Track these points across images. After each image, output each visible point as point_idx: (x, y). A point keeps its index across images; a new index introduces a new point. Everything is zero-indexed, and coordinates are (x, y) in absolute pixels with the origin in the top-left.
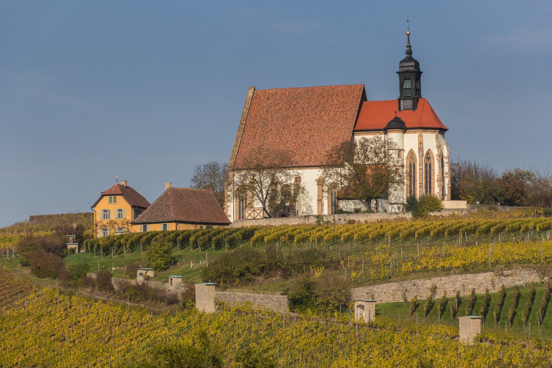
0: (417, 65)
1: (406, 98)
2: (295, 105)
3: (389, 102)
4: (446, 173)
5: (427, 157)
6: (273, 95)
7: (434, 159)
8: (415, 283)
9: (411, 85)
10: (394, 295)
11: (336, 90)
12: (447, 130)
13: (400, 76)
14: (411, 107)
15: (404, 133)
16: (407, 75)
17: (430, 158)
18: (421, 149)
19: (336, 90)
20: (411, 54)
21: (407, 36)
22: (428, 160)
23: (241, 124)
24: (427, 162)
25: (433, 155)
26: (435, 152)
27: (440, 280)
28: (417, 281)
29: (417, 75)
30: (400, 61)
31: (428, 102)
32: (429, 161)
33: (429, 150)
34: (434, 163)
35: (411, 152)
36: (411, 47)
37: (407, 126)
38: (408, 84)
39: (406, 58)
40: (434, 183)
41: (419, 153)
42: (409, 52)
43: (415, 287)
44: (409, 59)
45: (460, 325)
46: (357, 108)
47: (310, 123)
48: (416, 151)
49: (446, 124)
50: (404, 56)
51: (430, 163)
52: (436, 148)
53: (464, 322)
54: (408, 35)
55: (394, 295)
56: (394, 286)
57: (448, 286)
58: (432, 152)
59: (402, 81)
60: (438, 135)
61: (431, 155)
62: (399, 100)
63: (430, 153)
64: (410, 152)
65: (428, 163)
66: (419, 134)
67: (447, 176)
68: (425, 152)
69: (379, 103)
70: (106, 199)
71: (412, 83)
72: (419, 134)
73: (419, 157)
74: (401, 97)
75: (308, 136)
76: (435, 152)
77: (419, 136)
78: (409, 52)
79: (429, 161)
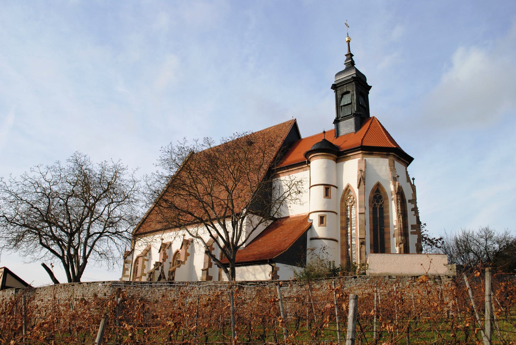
4: (412, 226)
5: (375, 197)
7: (387, 198)
13: (336, 92)
14: (353, 130)
15: (337, 161)
17: (380, 197)
18: (362, 180)
20: (352, 63)
21: (347, 44)
22: (378, 202)
24: (375, 205)
25: (385, 193)
26: (391, 188)
30: (336, 74)
31: (379, 122)
32: (380, 204)
33: (378, 185)
34: (388, 206)
35: (348, 190)
36: (352, 55)
39: (346, 68)
40: (389, 239)
41: (358, 188)
42: (351, 64)
51: (381, 205)
54: (349, 41)
58: (383, 188)
59: (338, 97)
60: (394, 162)
61: (382, 194)
63: (380, 189)
64: (346, 189)
65: (378, 207)
66: (359, 159)
67: (415, 230)
68: (371, 185)
71: (353, 95)
72: (359, 159)
73: (359, 194)
74: (337, 118)
76: (391, 188)
77: (359, 162)
78: (351, 64)
79: (380, 204)
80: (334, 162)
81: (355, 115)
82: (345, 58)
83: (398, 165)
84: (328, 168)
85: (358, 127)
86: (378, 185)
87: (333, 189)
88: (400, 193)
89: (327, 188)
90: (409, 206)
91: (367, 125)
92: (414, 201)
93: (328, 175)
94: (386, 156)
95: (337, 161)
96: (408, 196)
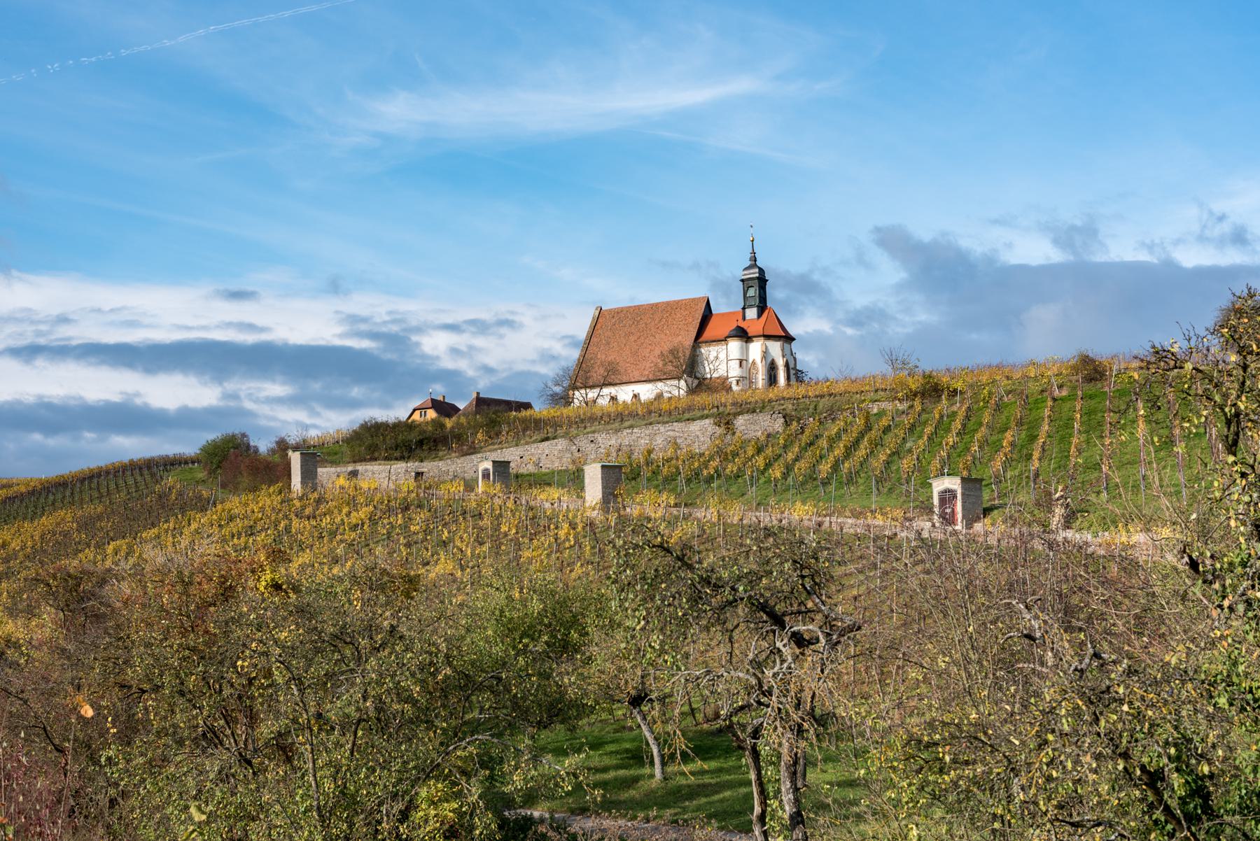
0: (761, 271)
1: (751, 306)
2: (638, 322)
3: (734, 313)
6: (618, 313)
8: (592, 439)
9: (755, 293)
10: (561, 458)
11: (680, 304)
12: (793, 339)
14: (756, 317)
15: (746, 342)
16: (751, 283)
19: (680, 304)
20: (755, 261)
23: (585, 344)
26: (780, 363)
27: (632, 433)
28: (596, 435)
29: (762, 281)
35: (754, 363)
37: (750, 335)
38: (751, 292)
43: (593, 445)
44: (754, 265)
45: (587, 481)
46: (699, 321)
47: (652, 338)
48: (758, 361)
49: (792, 331)
50: (748, 263)
52: (781, 358)
53: (591, 474)
55: (561, 458)
56: (561, 444)
57: (642, 441)
62: (744, 309)
69: (723, 315)
70: (418, 413)
75: (648, 350)
76: (780, 363)
77: (762, 345)
80: (744, 344)
81: (758, 306)
82: (750, 255)
83: (786, 345)
84: (742, 347)
85: (760, 315)
86: (773, 360)
87: (744, 362)
88: (787, 365)
89: (741, 361)
90: (792, 372)
91: (767, 312)
92: (795, 368)
93: (742, 353)
94: (779, 340)
95: (746, 342)
96: (791, 365)
